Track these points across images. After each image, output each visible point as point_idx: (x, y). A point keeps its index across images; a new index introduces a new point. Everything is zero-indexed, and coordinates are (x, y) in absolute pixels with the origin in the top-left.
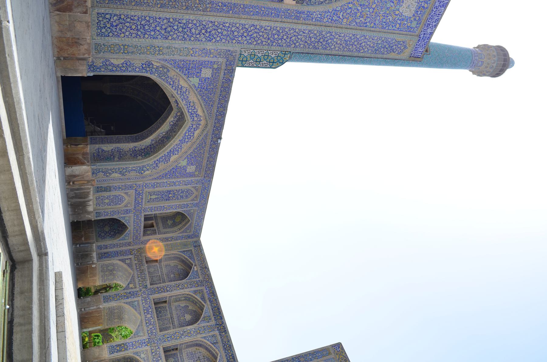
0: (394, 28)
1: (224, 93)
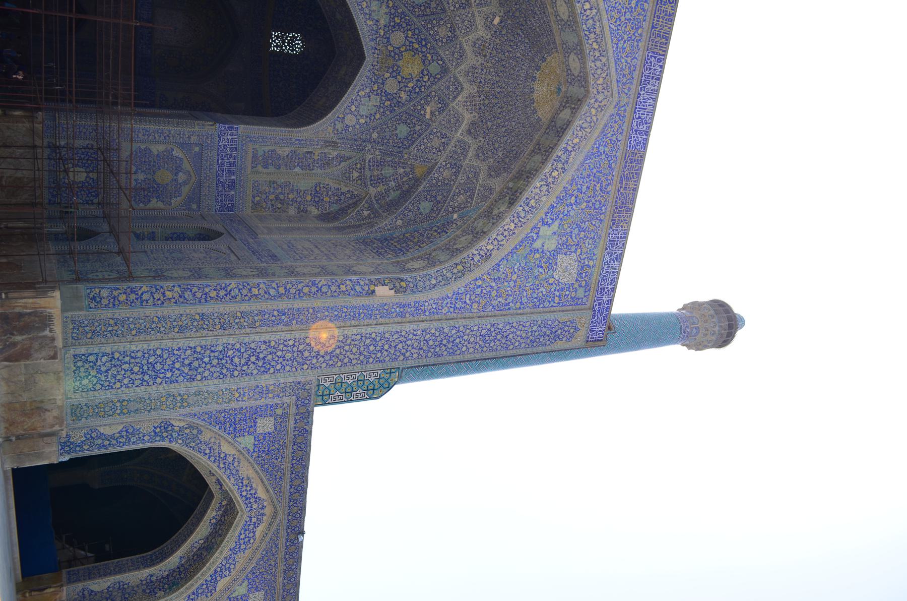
1: (299, 454)
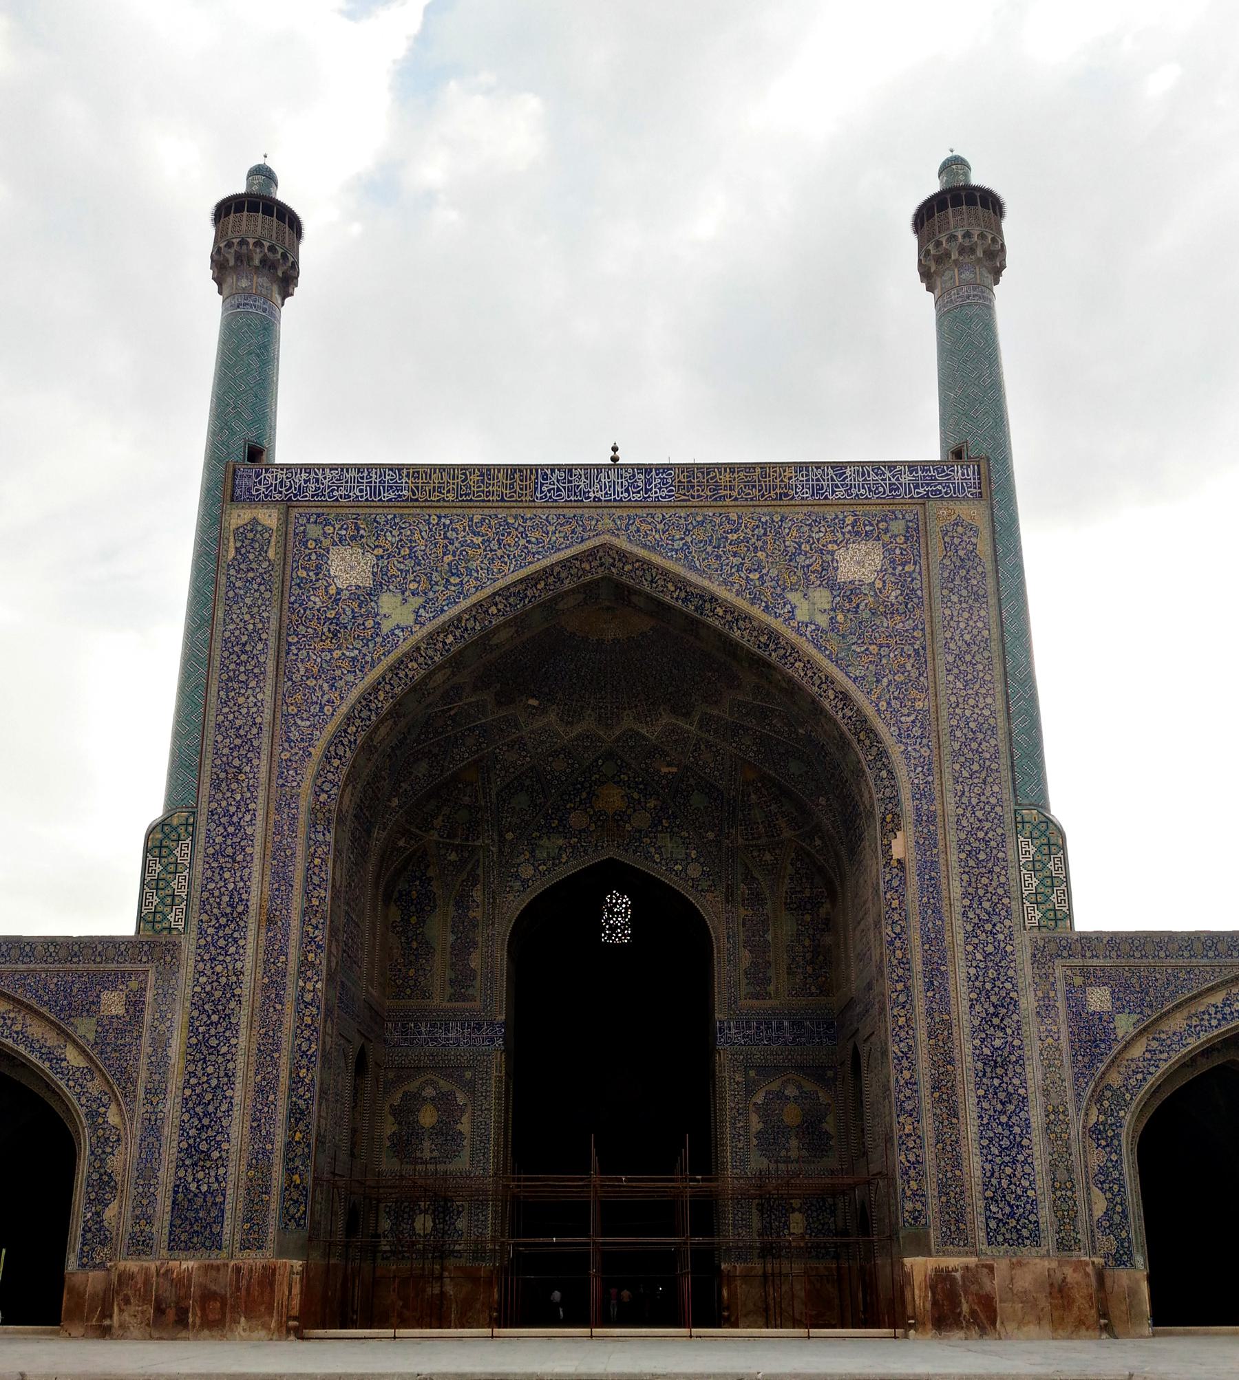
0: (916, 575)
